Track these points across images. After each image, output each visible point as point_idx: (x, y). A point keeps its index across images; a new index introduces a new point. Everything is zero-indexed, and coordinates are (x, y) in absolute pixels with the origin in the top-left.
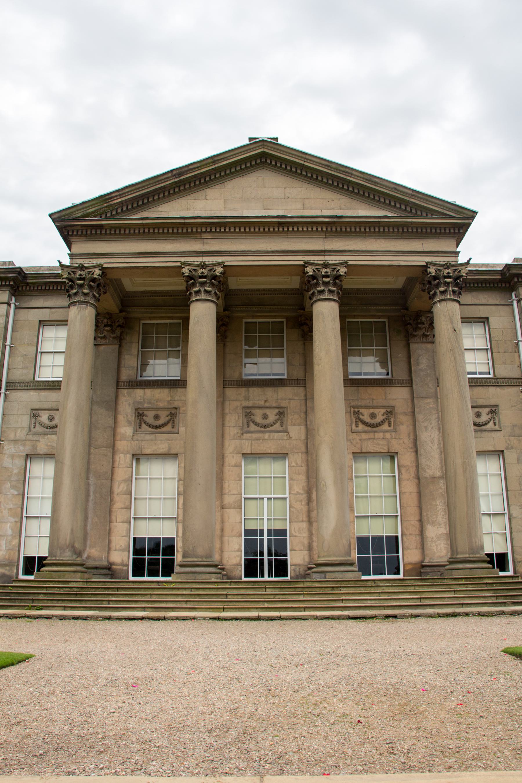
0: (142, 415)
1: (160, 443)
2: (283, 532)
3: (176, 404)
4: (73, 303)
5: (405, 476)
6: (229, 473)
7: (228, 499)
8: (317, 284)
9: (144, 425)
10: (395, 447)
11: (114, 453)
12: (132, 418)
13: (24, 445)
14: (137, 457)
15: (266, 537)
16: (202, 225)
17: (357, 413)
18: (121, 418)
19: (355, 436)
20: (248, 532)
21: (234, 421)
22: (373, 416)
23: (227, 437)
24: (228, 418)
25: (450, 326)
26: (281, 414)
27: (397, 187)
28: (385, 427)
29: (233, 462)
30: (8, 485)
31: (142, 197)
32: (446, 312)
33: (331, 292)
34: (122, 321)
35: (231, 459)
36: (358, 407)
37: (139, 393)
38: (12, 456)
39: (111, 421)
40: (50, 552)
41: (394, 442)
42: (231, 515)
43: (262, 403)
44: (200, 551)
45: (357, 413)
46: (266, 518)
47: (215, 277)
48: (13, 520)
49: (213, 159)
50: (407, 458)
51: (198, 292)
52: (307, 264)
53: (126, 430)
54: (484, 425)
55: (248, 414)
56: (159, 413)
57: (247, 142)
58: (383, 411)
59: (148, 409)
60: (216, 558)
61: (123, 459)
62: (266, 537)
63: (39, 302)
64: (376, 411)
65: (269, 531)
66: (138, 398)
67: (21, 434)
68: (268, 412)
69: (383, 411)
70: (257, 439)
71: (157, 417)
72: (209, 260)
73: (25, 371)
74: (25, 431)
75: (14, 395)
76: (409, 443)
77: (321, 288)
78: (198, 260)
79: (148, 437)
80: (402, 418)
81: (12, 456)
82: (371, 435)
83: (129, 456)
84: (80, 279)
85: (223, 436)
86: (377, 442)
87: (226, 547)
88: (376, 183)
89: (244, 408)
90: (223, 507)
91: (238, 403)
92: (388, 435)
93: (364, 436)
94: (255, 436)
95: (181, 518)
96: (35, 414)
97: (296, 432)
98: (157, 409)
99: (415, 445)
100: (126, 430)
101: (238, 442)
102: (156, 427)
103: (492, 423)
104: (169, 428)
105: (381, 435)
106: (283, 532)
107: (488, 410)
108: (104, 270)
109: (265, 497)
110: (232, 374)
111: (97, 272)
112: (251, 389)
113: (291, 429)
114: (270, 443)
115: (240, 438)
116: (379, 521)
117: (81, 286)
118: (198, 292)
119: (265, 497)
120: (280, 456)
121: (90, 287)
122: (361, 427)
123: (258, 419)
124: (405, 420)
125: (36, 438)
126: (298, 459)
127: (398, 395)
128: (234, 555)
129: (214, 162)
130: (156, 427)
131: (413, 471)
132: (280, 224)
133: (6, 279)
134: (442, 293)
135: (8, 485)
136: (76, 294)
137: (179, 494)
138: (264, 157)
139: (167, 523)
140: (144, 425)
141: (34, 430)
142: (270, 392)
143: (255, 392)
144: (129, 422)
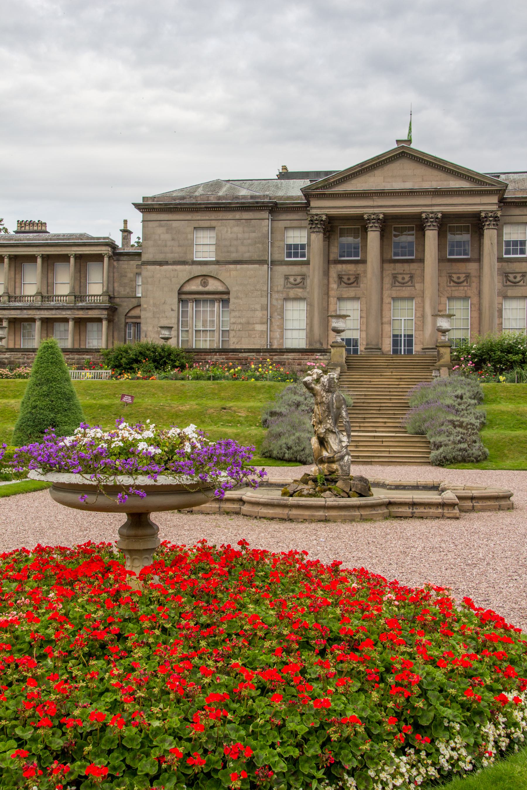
0: (342, 278)
1: (351, 292)
2: (411, 336)
3: (358, 272)
4: (313, 232)
5: (473, 309)
6: (385, 307)
7: (385, 320)
8: (427, 222)
9: (342, 283)
10: (469, 293)
11: (328, 297)
12: (336, 279)
13: (282, 294)
14: (340, 299)
15: (403, 338)
16: (373, 193)
17: (450, 277)
18: (331, 280)
19: (449, 288)
20: (394, 336)
21: (388, 280)
22: (459, 278)
23: (384, 289)
24: (385, 279)
25: (490, 242)
26: (412, 277)
27: (469, 171)
28: (465, 284)
29: (387, 302)
30: (276, 314)
31: (344, 178)
32: (490, 235)
33: (434, 226)
34: (329, 229)
35: (387, 300)
36: (451, 273)
37: (339, 267)
38: (277, 299)
39: (326, 281)
40: (310, 344)
41: (469, 292)
42: (386, 328)
43: (402, 271)
44: (374, 343)
45: (450, 277)
46: (403, 329)
47: (379, 219)
48: (279, 330)
49: (378, 157)
50: (475, 300)
51: (371, 227)
52: (422, 213)
53: (334, 286)
54: (518, 282)
55: (395, 277)
56: (350, 277)
57: (395, 146)
58: (464, 275)
59: (345, 275)
60: (380, 346)
61: (333, 300)
62: (403, 338)
63: (284, 217)
64: (460, 275)
65: (405, 335)
66: (339, 269)
67: (280, 288)
68: (405, 276)
69: (464, 275)
70: (399, 290)
71: (349, 279)
72: (376, 210)
73: (280, 255)
74: (282, 287)
76: (476, 291)
77: (429, 224)
79: (345, 289)
80: (474, 279)
81: (277, 299)
82: (457, 288)
83: (335, 299)
84: (316, 220)
85: (382, 289)
86: (460, 291)
87: (384, 343)
88: (458, 169)
89: (393, 274)
90: (382, 324)
91: (389, 272)
92: (466, 288)
93: (453, 288)
94: (398, 288)
95: (364, 328)
96: (287, 277)
97: (418, 286)
98: (349, 275)
99: (480, 293)
100: (334, 286)
101: (389, 292)
102: (349, 284)
103: (522, 282)
104: (355, 284)
105: (462, 288)
106: (411, 336)
107: (521, 275)
108: (327, 215)
109: (403, 319)
110: (387, 256)
111: (324, 218)
112: (397, 264)
113: (416, 285)
114: (406, 292)
115: (391, 290)
116: (459, 331)
117: (317, 224)
118: (371, 227)
119: (403, 318)
120: (411, 298)
121: (321, 224)
122: (452, 284)
123: (400, 280)
124: (475, 280)
125: (288, 290)
126: (419, 300)
127: (472, 267)
128: (387, 346)
129: (379, 159)
130: (349, 284)
131: (477, 306)
132: (410, 192)
133: (267, 206)
134: (488, 225)
135: (276, 314)
136: (314, 228)
137: (361, 317)
138: (403, 153)
139: (355, 331)
140: (342, 283)
141: (286, 286)
142: (406, 266)
143: (398, 266)
144: (335, 282)
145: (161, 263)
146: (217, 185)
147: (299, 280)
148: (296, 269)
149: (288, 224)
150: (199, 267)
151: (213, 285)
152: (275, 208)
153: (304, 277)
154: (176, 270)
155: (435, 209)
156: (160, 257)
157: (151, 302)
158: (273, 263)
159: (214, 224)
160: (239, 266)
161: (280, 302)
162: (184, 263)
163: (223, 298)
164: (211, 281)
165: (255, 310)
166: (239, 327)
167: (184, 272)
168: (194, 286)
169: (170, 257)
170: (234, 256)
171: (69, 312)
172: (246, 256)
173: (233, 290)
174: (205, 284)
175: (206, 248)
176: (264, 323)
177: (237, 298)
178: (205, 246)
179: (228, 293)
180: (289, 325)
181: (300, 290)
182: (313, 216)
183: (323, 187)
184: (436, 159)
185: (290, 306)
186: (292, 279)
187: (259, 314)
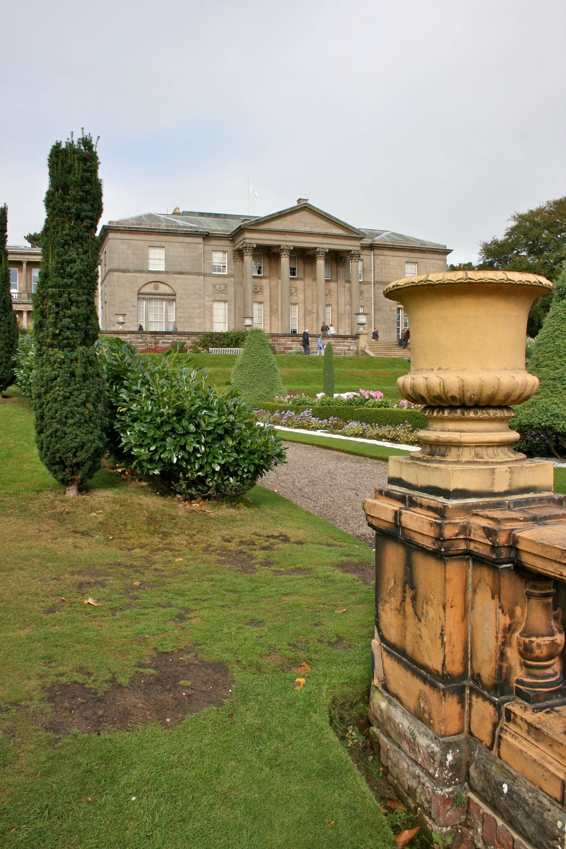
27: (345, 224)
38: (208, 301)
49: (291, 208)
50: (335, 307)
67: (210, 293)
72: (289, 244)
75: (207, 279)
78: (285, 243)
81: (208, 301)
96: (214, 286)
138: (304, 207)
145: (123, 271)
146: (151, 217)
147: (223, 287)
148: (219, 280)
149: (214, 248)
150: (153, 275)
151: (163, 289)
152: (207, 236)
153: (226, 286)
154: (135, 277)
155: (325, 246)
156: (123, 267)
157: (117, 300)
158: (205, 275)
159: (163, 244)
160: (182, 276)
161: (210, 303)
162: (142, 272)
163: (171, 298)
164: (161, 285)
165: (194, 308)
166: (183, 319)
167: (142, 278)
168: (149, 289)
169: (130, 267)
170: (178, 269)
171: (23, 306)
172: (187, 269)
173: (179, 292)
174: (157, 288)
175: (157, 262)
176: (201, 318)
177: (181, 298)
178: (157, 260)
179: (175, 295)
180: (215, 319)
181: (224, 295)
182: (247, 243)
183: (254, 225)
184: (326, 214)
185: (216, 305)
186: (218, 287)
187: (197, 311)
